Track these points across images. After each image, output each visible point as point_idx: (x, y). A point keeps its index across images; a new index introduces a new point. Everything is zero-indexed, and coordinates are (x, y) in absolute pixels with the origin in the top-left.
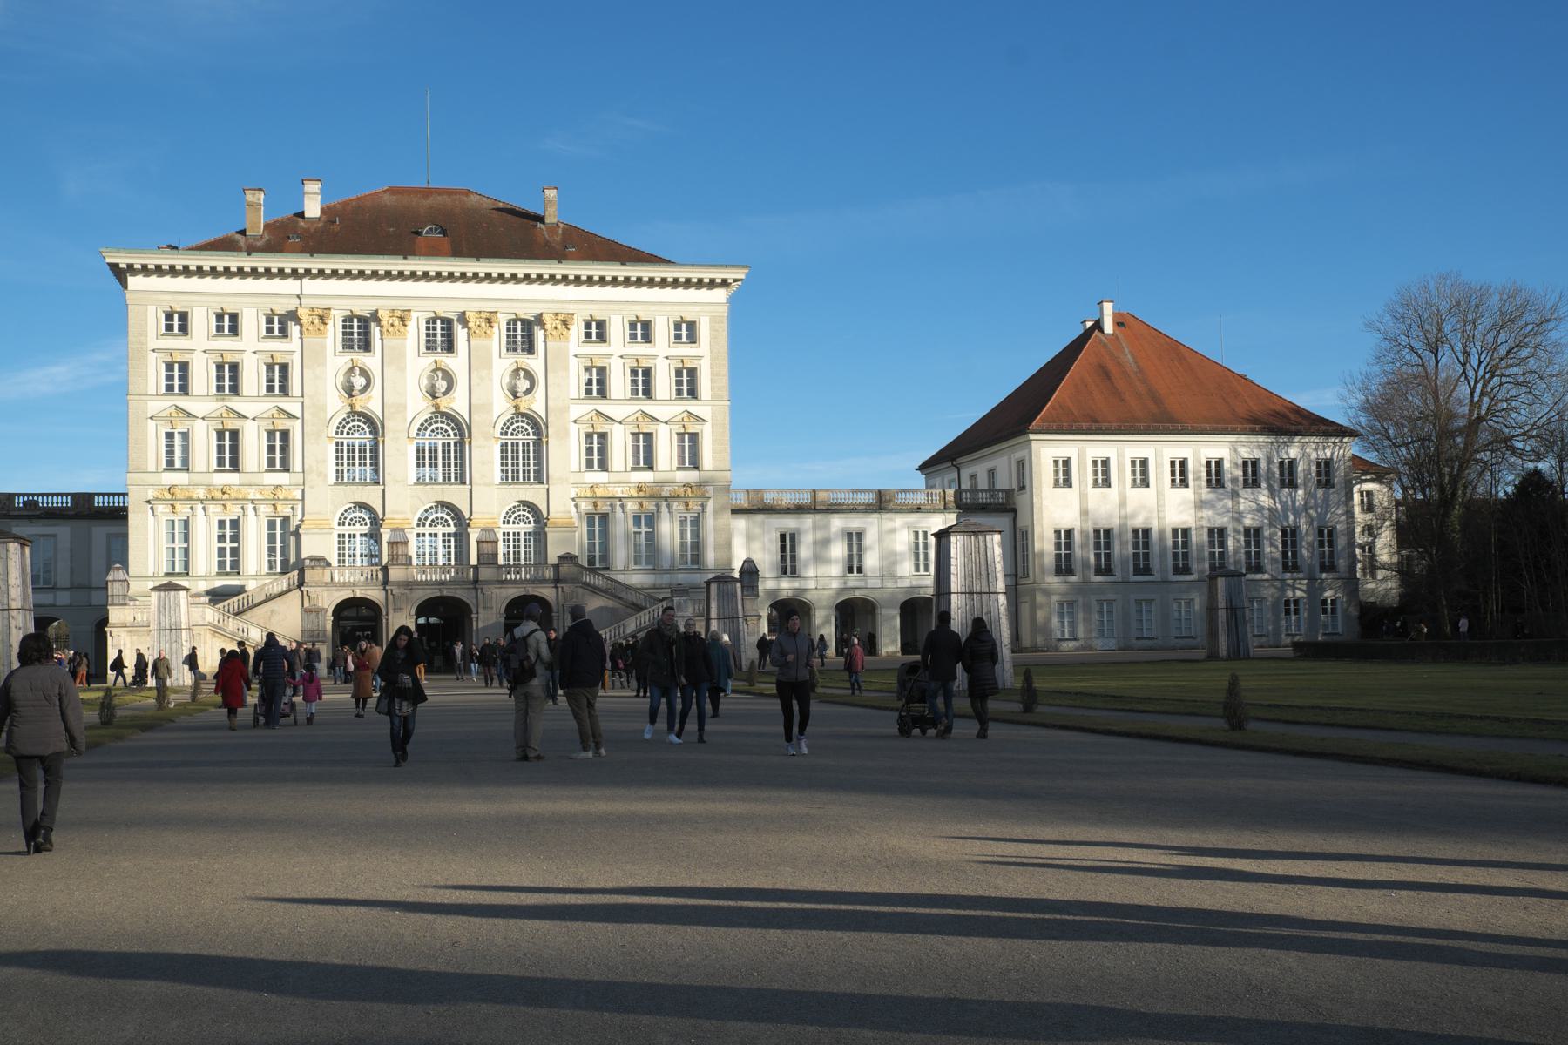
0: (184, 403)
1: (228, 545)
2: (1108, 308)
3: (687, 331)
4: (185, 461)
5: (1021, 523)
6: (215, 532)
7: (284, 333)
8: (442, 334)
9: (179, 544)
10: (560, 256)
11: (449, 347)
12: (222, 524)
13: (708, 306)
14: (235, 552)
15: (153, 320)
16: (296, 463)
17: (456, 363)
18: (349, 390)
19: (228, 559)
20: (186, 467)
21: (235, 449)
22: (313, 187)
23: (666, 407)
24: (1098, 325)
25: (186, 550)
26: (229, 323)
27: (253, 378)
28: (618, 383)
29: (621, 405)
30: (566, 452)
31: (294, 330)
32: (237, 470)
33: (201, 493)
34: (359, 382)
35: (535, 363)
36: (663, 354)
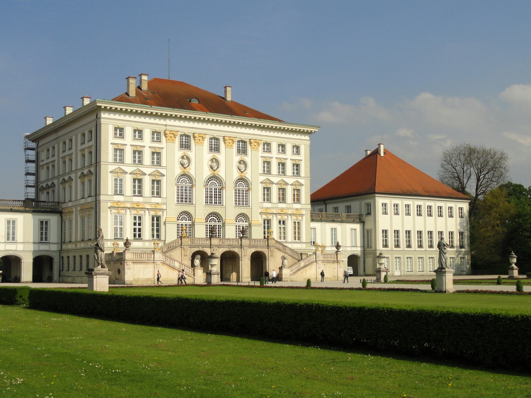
1: (137, 227)
3: (297, 149)
4: (121, 191)
5: (368, 226)
6: (133, 221)
7: (159, 140)
9: (118, 226)
12: (135, 218)
13: (304, 141)
14: (140, 230)
16: (164, 193)
17: (221, 157)
19: (137, 233)
20: (121, 194)
21: (140, 187)
22: (145, 78)
24: (376, 152)
25: (121, 229)
27: (147, 158)
31: (163, 138)
32: (141, 196)
33: (129, 205)
35: (247, 159)
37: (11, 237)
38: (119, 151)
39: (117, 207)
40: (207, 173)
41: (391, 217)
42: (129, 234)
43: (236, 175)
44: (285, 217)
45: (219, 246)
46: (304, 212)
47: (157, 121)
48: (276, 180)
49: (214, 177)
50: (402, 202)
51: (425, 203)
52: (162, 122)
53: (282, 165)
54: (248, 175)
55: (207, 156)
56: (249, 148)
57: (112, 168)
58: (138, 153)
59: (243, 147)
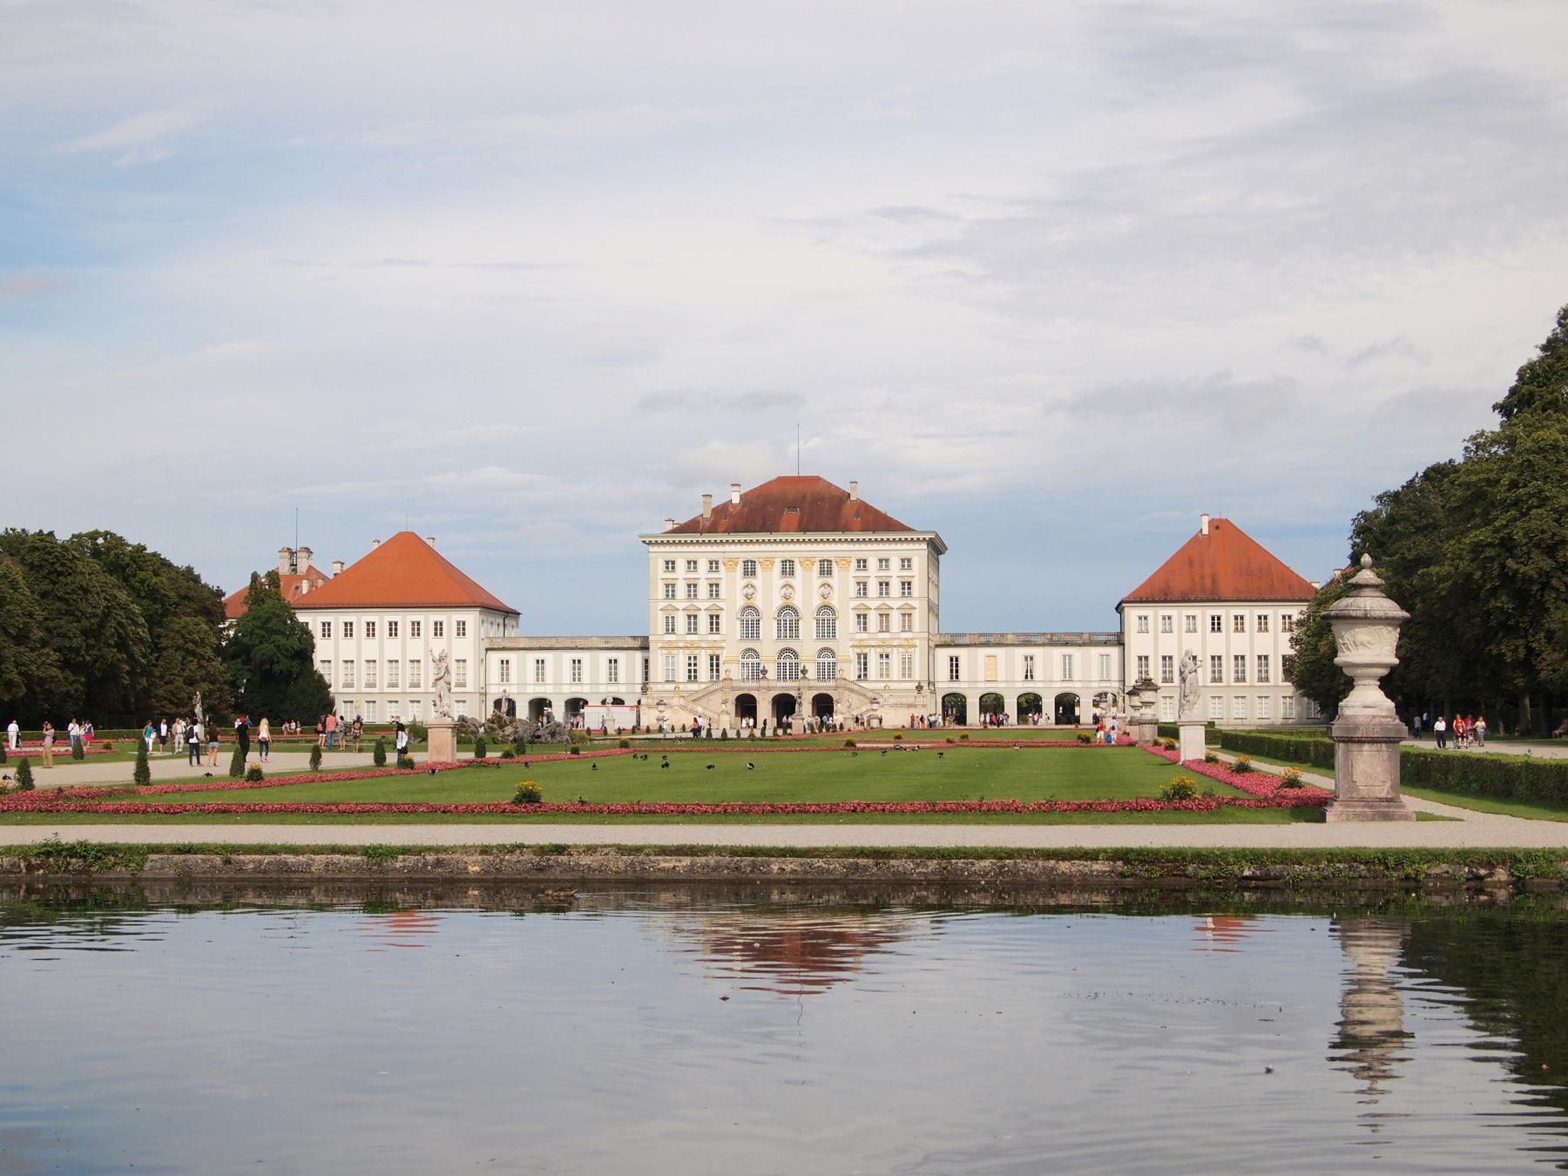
0: (674, 603)
2: (1206, 520)
3: (906, 563)
8: (788, 568)
10: (844, 531)
11: (792, 573)
15: (661, 565)
17: (796, 581)
18: (748, 597)
23: (895, 599)
26: (692, 564)
27: (703, 590)
28: (873, 589)
29: (873, 601)
30: (846, 624)
31: (721, 566)
34: (750, 591)
36: (895, 573)
37: (613, 677)
38: (670, 589)
39: (669, 647)
40: (779, 602)
41: (1156, 638)
42: (682, 675)
43: (817, 602)
44: (888, 650)
45: (769, 689)
46: (917, 642)
47: (715, 548)
48: (873, 604)
49: (788, 608)
50: (1179, 613)
51: (1227, 612)
52: (721, 548)
53: (884, 585)
54: (834, 602)
55: (777, 580)
56: (835, 568)
57: (662, 605)
58: (692, 586)
59: (826, 568)
